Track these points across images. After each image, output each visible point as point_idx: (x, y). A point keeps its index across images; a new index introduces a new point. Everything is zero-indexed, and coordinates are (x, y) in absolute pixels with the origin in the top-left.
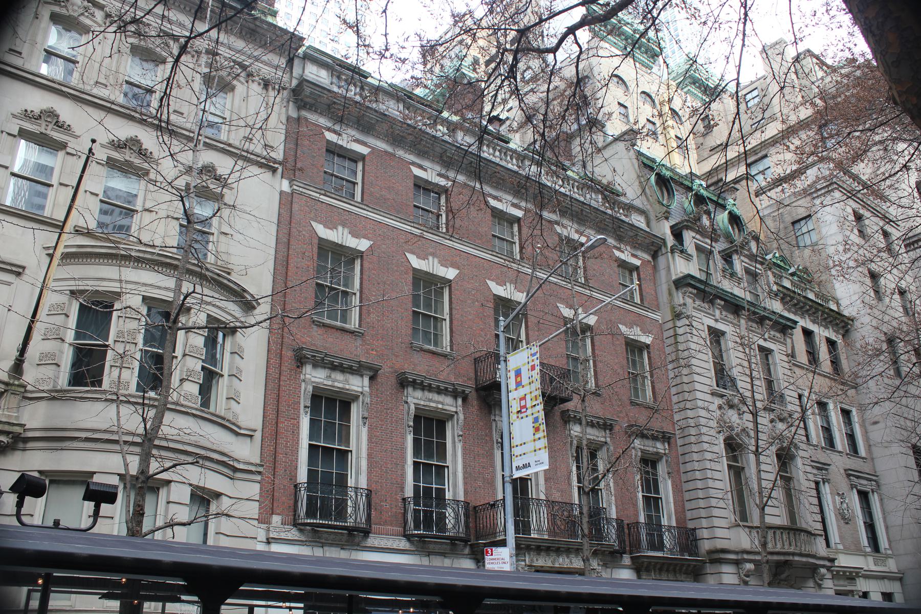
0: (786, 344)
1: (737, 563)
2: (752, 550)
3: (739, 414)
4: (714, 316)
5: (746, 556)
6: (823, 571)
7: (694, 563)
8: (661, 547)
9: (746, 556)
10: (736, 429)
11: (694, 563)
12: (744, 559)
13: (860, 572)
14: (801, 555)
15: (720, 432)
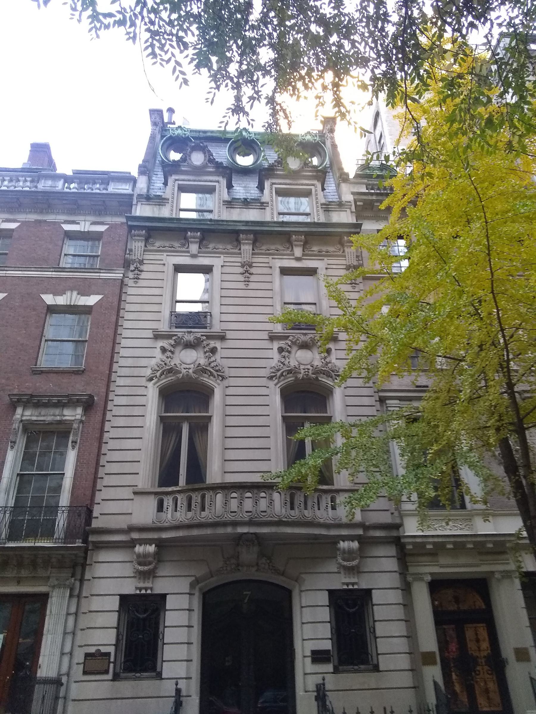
0: (345, 256)
1: (131, 544)
2: (159, 524)
3: (205, 353)
4: (188, 252)
5: (135, 535)
6: (343, 545)
7: (62, 552)
8: (49, 533)
9: (135, 535)
10: (184, 371)
11: (62, 552)
12: (136, 540)
13: (510, 541)
14: (251, 523)
15: (151, 379)
